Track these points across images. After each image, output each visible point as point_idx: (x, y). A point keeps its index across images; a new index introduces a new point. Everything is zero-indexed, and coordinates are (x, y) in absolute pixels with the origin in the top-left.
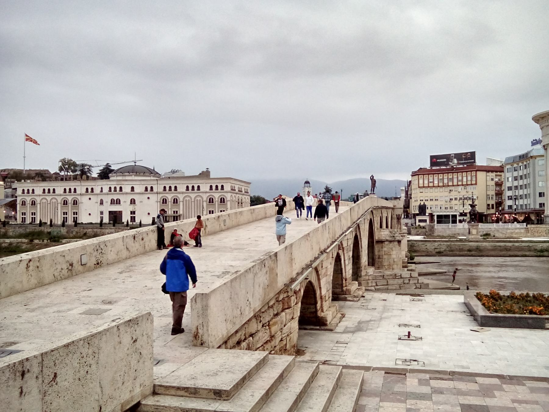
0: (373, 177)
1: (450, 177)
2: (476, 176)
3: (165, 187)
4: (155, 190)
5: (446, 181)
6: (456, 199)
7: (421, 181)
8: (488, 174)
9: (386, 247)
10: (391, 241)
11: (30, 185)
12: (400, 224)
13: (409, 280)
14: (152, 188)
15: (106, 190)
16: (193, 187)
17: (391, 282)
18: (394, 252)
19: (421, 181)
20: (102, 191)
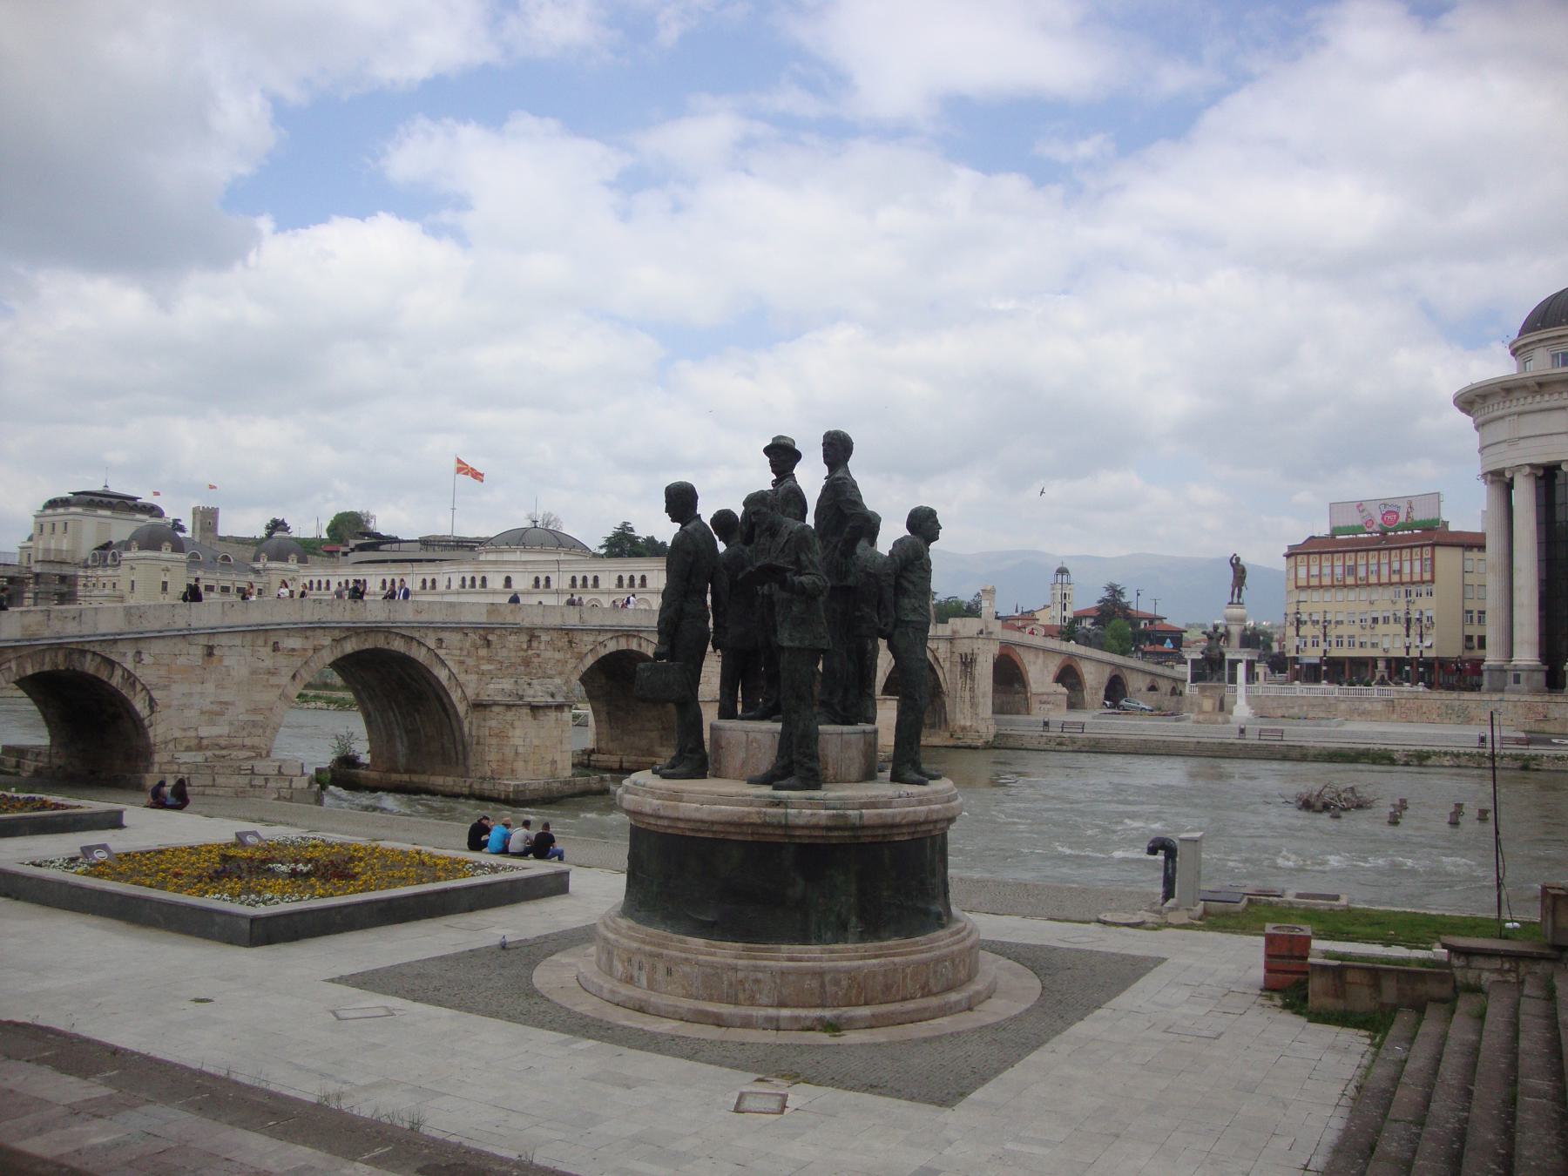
0: (1238, 559)
1: (1349, 563)
2: (1433, 559)
3: (574, 579)
4: (554, 585)
5: (1362, 572)
6: (1386, 620)
7: (1302, 572)
8: (1468, 554)
9: (494, 720)
10: (509, 707)
11: (320, 571)
12: (973, 679)
13: (267, 780)
14: (548, 579)
15: (456, 585)
16: (632, 579)
17: (220, 780)
18: (518, 732)
19: (1302, 572)
20: (449, 587)
